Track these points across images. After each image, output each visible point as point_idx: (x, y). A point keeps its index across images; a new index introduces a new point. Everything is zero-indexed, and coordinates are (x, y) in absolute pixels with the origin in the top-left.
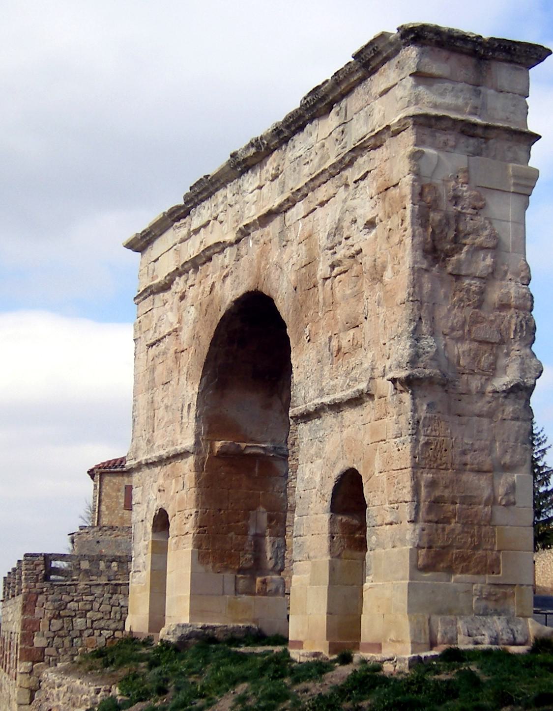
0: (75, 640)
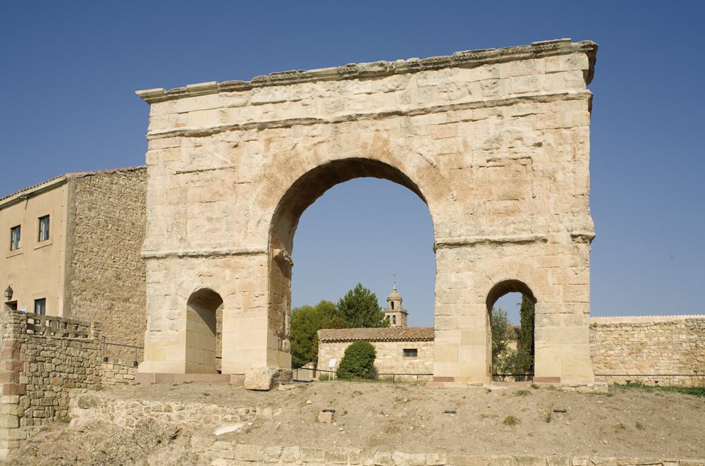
0: (45, 379)
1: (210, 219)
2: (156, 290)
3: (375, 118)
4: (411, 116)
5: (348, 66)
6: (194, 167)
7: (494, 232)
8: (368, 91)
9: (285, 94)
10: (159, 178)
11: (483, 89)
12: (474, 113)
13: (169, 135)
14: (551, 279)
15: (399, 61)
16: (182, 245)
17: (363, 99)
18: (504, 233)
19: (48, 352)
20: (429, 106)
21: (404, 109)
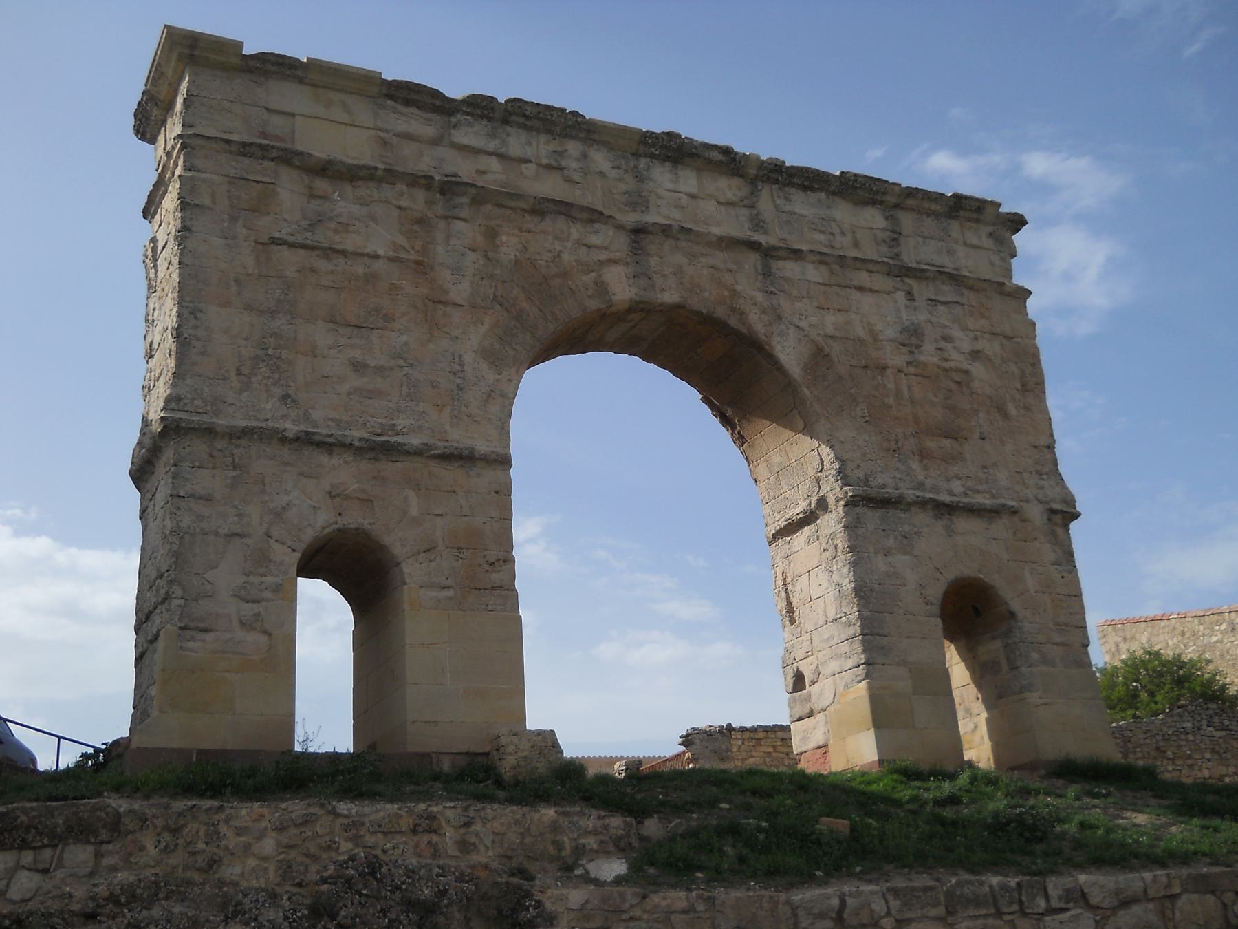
1: (358, 367)
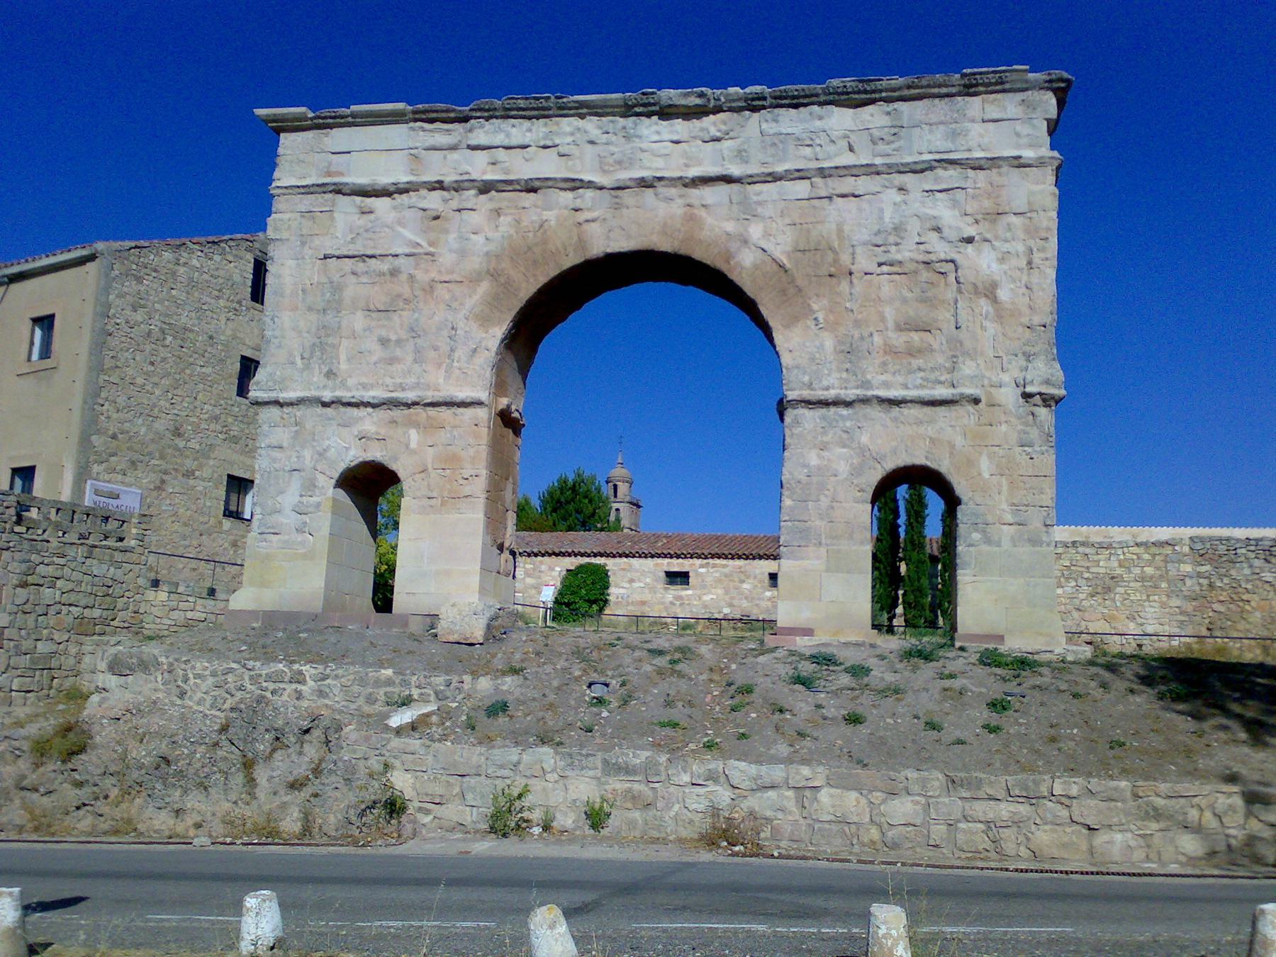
2: (274, 460)
3: (685, 186)
4: (750, 184)
5: (644, 94)
6: (358, 248)
7: (886, 385)
8: (675, 138)
9: (528, 134)
10: (291, 263)
11: (874, 143)
12: (859, 182)
13: (312, 190)
14: (985, 466)
15: (732, 90)
16: (330, 383)
17: (663, 151)
18: (906, 387)
19: (50, 568)
20: (780, 168)
21: (735, 171)
